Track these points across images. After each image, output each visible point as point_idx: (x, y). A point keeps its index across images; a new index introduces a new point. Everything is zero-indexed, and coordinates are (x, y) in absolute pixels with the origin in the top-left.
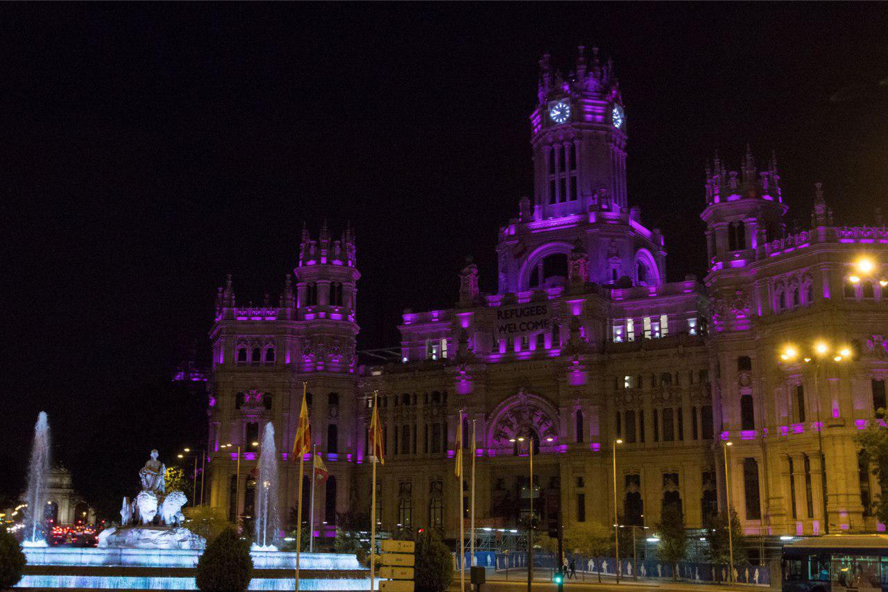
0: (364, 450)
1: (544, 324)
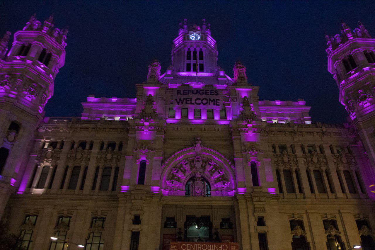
0: (28, 182)
1: (216, 102)
